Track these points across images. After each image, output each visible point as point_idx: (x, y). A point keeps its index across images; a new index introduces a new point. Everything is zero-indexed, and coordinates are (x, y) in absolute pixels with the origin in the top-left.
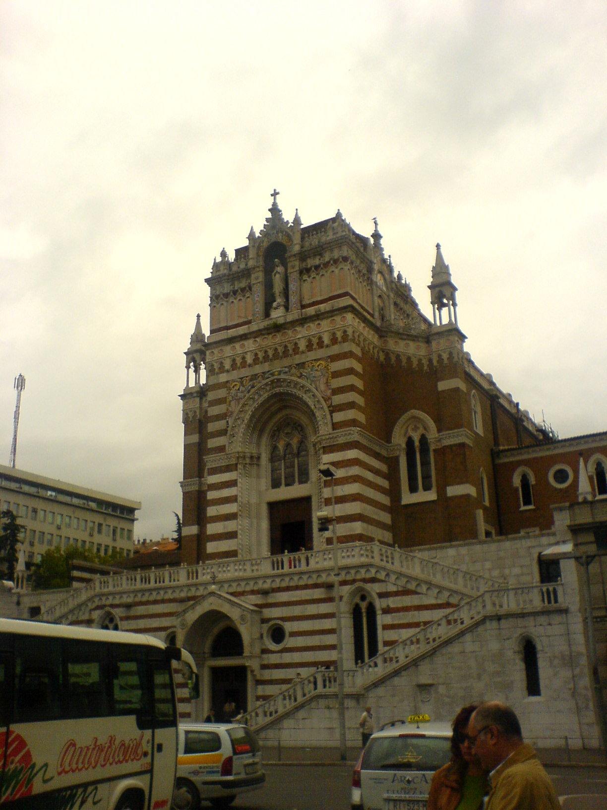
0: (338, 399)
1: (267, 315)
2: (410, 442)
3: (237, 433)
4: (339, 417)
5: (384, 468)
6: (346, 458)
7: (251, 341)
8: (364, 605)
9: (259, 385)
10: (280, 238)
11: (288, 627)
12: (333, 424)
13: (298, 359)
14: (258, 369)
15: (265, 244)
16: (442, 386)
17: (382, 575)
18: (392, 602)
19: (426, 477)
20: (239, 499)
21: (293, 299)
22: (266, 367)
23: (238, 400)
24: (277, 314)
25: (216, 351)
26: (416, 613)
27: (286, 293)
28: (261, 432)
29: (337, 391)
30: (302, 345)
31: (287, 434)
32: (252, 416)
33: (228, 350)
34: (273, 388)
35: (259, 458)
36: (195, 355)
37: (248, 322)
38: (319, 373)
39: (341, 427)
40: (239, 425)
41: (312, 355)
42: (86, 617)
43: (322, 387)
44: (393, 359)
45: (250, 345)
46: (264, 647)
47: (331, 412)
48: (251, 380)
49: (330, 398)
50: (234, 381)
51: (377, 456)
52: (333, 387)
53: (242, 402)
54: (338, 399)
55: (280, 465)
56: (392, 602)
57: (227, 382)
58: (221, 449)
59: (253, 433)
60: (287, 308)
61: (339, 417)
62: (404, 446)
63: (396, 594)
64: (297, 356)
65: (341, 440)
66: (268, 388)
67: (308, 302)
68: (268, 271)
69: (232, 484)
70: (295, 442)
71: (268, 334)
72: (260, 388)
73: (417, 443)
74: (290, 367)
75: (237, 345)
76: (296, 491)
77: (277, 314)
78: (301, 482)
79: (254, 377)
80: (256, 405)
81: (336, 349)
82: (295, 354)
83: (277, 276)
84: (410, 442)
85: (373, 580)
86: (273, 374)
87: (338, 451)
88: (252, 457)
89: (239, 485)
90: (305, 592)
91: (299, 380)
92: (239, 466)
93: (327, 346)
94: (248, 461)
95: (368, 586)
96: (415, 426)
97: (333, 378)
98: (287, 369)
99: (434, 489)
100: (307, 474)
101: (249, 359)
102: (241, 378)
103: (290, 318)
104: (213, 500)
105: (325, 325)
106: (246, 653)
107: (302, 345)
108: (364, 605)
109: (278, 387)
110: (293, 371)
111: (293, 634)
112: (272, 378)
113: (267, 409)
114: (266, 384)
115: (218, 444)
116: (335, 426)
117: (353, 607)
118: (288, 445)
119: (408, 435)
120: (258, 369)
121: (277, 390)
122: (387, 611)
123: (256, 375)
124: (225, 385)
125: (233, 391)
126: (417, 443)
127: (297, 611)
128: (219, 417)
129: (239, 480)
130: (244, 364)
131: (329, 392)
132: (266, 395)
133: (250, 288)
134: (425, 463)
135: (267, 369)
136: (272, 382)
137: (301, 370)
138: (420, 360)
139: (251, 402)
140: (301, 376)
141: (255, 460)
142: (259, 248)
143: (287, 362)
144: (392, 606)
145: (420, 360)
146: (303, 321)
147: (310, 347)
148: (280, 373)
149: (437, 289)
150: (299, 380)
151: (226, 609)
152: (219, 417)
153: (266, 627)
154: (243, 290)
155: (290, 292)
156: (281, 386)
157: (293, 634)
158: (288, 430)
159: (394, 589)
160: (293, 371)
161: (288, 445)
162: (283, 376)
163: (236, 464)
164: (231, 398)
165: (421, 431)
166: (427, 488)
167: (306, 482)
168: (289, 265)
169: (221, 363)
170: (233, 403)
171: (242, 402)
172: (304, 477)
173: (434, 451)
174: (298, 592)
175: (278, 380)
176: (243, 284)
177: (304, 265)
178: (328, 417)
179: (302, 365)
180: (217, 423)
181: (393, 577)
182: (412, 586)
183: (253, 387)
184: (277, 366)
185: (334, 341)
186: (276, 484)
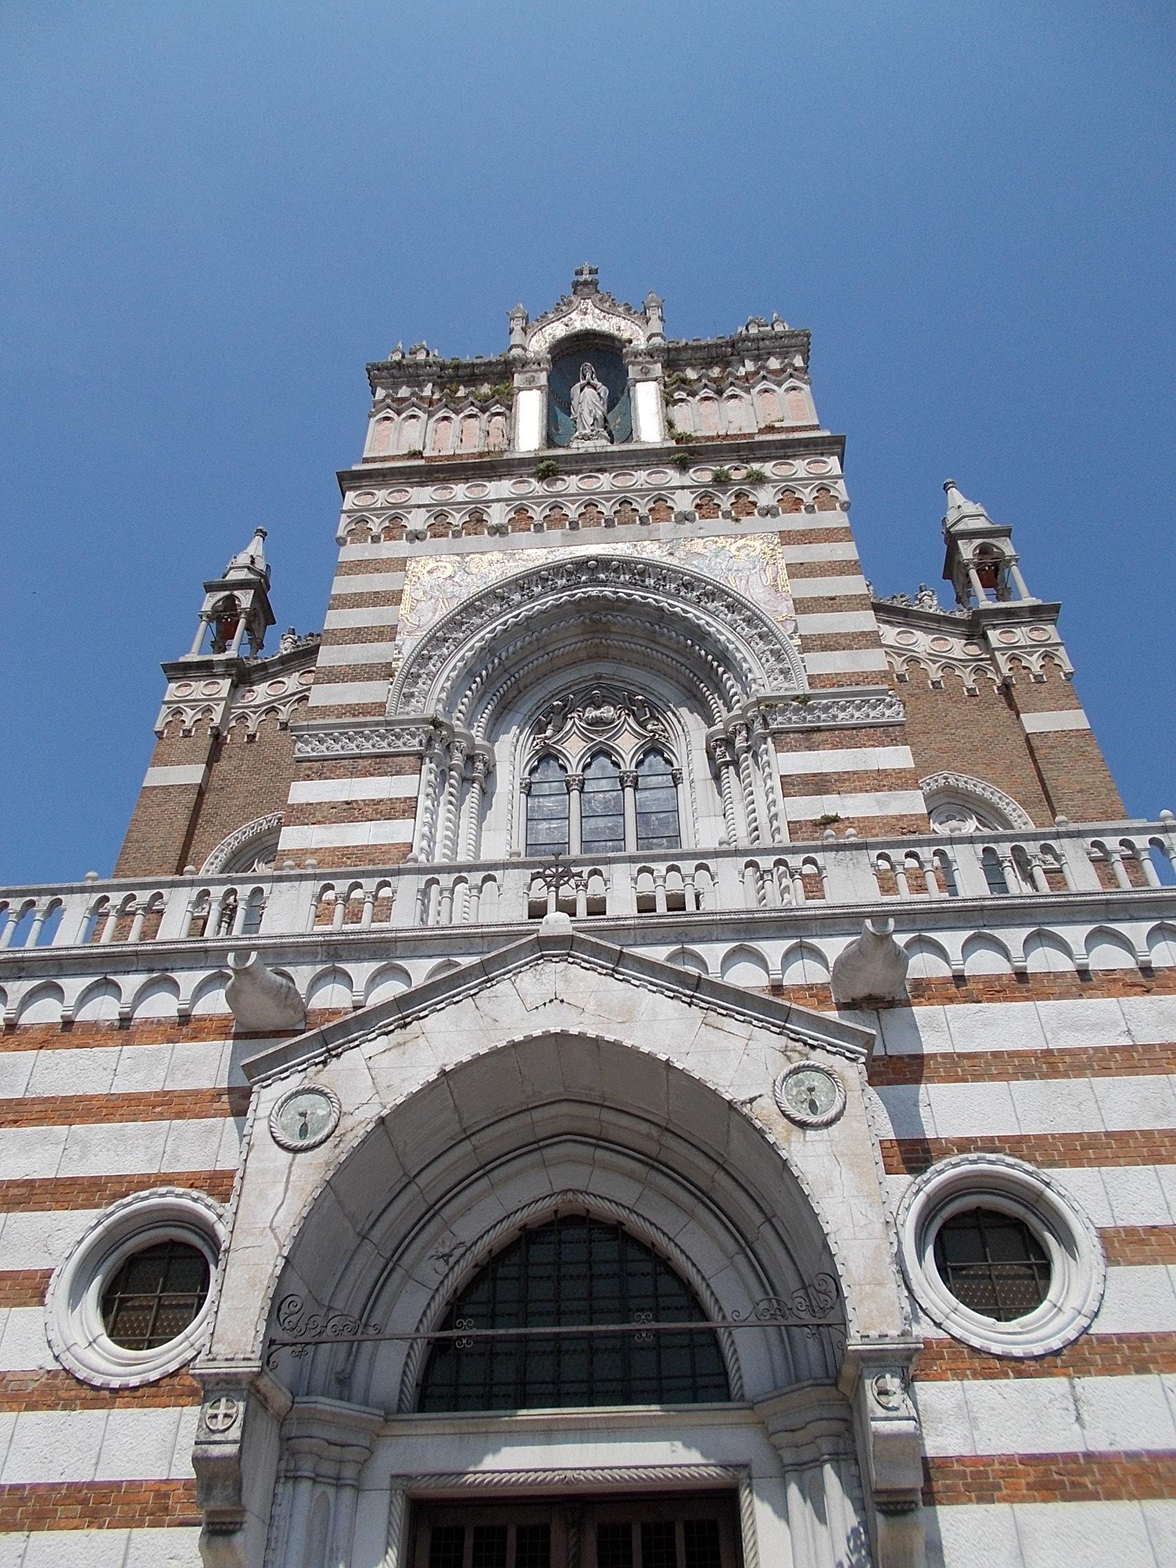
3: (432, 676)
11: (1085, 1197)
16: (1033, 722)
31: (598, 722)
34: (578, 585)
40: (443, 659)
59: (480, 698)
80: (509, 618)
88: (470, 759)
92: (428, 765)
94: (458, 759)
111: (1125, 1245)
121: (594, 591)
127: (1123, 1103)
129: (423, 803)
149: (979, 541)
151: (657, 1026)
153: (908, 1195)
156: (603, 583)
157: (1125, 1245)
158: (607, 712)
163: (421, 757)
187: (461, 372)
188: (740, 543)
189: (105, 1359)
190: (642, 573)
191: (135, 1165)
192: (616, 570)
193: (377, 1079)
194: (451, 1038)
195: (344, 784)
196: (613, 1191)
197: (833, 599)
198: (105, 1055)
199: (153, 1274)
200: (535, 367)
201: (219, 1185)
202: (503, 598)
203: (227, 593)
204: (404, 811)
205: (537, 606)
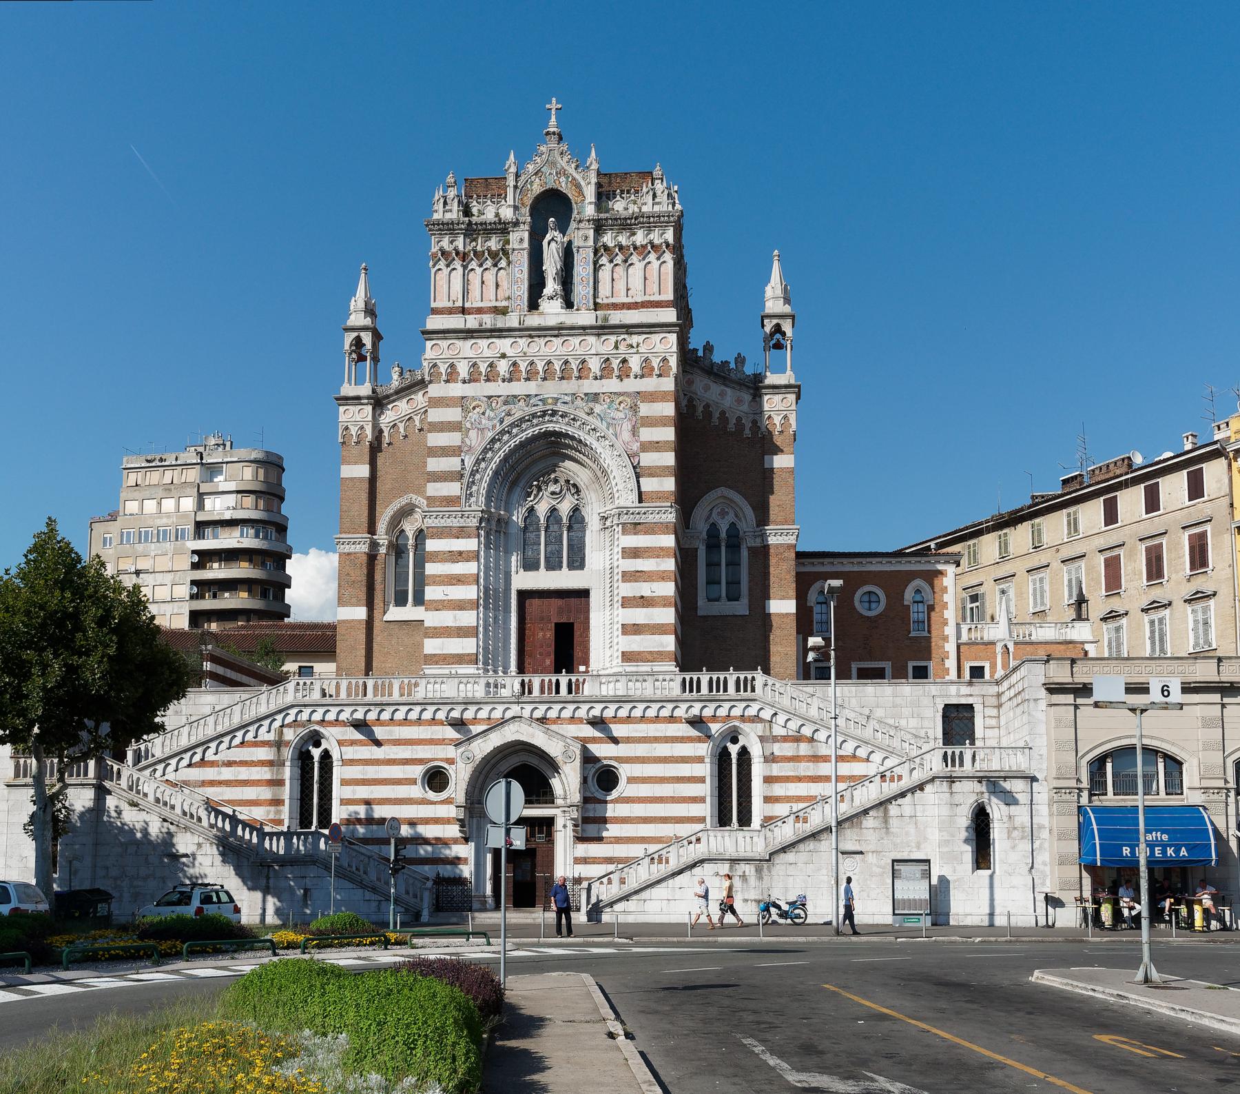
1: (533, 305)
2: (713, 531)
8: (734, 750)
11: (624, 771)
12: (640, 493)
13: (589, 386)
14: (518, 388)
17: (766, 714)
18: (778, 749)
19: (734, 583)
21: (581, 290)
22: (532, 388)
26: (811, 764)
27: (566, 279)
31: (553, 493)
32: (505, 459)
33: (466, 348)
36: (362, 334)
38: (621, 415)
41: (612, 385)
42: (271, 737)
43: (626, 436)
46: (588, 794)
47: (638, 476)
48: (506, 403)
49: (636, 455)
53: (490, 435)
54: (647, 459)
55: (539, 537)
56: (778, 749)
57: (463, 398)
60: (569, 304)
62: (704, 535)
63: (785, 739)
65: (651, 518)
67: (606, 301)
68: (536, 237)
70: (565, 508)
72: (522, 420)
73: (723, 535)
76: (564, 579)
77: (552, 311)
78: (571, 567)
79: (511, 400)
80: (512, 444)
81: (649, 384)
84: (713, 531)
85: (756, 719)
86: (544, 401)
87: (645, 533)
90: (652, 726)
95: (746, 727)
96: (723, 510)
97: (643, 425)
98: (568, 399)
99: (745, 600)
100: (583, 559)
102: (489, 397)
106: (559, 802)
108: (734, 750)
110: (579, 402)
111: (631, 780)
114: (534, 416)
117: (719, 750)
118: (553, 510)
119: (711, 521)
120: (518, 388)
122: (770, 759)
123: (515, 397)
124: (462, 401)
125: (474, 415)
126: (723, 535)
128: (445, 452)
131: (635, 447)
134: (733, 564)
136: (544, 413)
137: (591, 405)
138: (739, 419)
140: (590, 413)
144: (777, 753)
145: (739, 419)
147: (606, 371)
149: (775, 321)
150: (590, 418)
152: (445, 452)
154: (494, 255)
155: (576, 279)
156: (557, 422)
157: (631, 780)
159: (783, 732)
160: (579, 402)
161: (553, 510)
162: (560, 407)
164: (468, 425)
165: (731, 518)
166: (733, 597)
167: (581, 566)
169: (452, 366)
170: (473, 434)
172: (578, 562)
173: (749, 549)
174: (642, 726)
175: (554, 413)
179: (595, 397)
181: (781, 719)
182: (807, 731)
183: (509, 414)
184: (552, 389)
188: (621, 399)
189: (431, 795)
190: (574, 419)
191: (429, 756)
192: (562, 416)
193: (483, 748)
194: (496, 740)
196: (534, 761)
198: (415, 728)
199: (436, 779)
201: (451, 761)
205: (523, 436)
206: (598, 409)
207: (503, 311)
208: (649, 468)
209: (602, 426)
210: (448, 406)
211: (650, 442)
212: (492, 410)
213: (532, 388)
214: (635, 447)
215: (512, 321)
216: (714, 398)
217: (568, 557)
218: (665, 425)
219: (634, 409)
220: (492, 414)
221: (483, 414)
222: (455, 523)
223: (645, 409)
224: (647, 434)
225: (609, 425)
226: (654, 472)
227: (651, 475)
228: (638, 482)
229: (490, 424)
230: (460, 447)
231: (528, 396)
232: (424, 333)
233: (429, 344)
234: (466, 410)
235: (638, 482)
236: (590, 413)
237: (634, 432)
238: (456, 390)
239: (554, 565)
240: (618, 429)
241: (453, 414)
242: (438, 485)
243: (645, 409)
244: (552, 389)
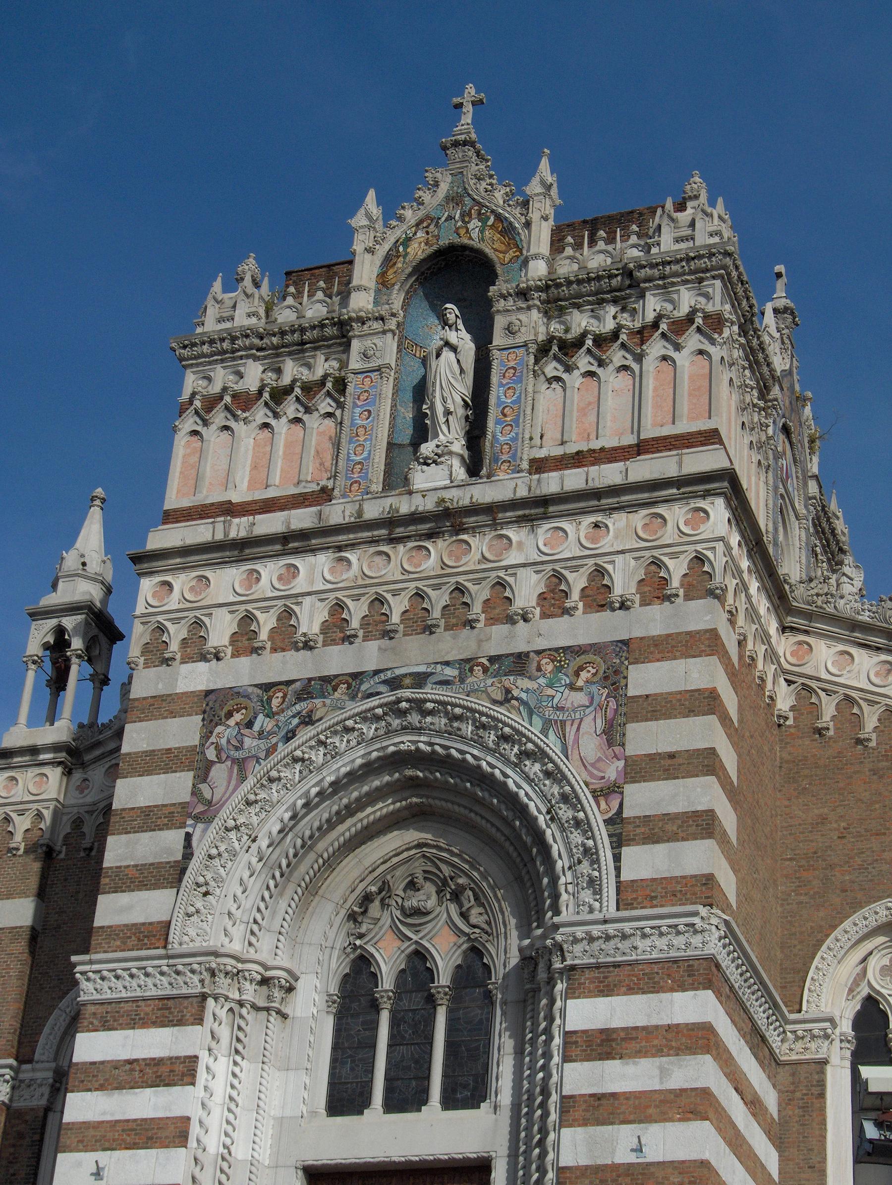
0: (643, 799)
4: (643, 862)
5: (771, 1099)
6: (665, 1020)
7: (323, 561)
9: (338, 716)
10: (477, 235)
13: (500, 640)
15: (418, 250)
20: (195, 1130)
23: (241, 765)
24: (437, 480)
25: (181, 582)
28: (311, 890)
29: (644, 769)
30: (527, 590)
33: (226, 581)
35: (290, 989)
37: (324, 495)
38: (580, 698)
39: (652, 900)
43: (590, 744)
44: (829, 708)
45: (315, 569)
47: (618, 842)
50: (233, 693)
51: (757, 1040)
52: (631, 750)
54: (643, 799)
55: (374, 1026)
57: (208, 693)
58: (157, 934)
61: (643, 862)
62: (846, 1027)
64: (499, 630)
66: (369, 730)
69: (179, 1071)
71: (393, 541)
74: (467, 664)
75: (269, 571)
82: (492, 621)
83: (448, 355)
86: (394, 683)
87: (631, 990)
89: (202, 1076)
91: (501, 712)
93: (623, 606)
98: (450, 672)
101: (311, 619)
102: (267, 687)
103: (485, 493)
104: (86, 1125)
105: (623, 528)
107: (527, 590)
109: (407, 729)
110: (477, 678)
112: (389, 697)
113: (351, 810)
115: (137, 917)
116: (630, 894)
120: (337, 660)
121: (406, 742)
123: (326, 680)
128: (151, 819)
130: (287, 637)
131: (613, 771)
132: (356, 757)
133: (341, 385)
135: (371, 667)
137: (509, 681)
139: (291, 773)
141: (276, 986)
142: (389, 260)
143: (453, 645)
146: (536, 509)
148: (420, 680)
150: (501, 712)
152: (151, 819)
156: (419, 730)
162: (430, 692)
163: (204, 997)
168: (500, 322)
170: (219, 773)
171: (255, 772)
175: (418, 705)
176: (323, 365)
177: (556, 328)
178: (606, 855)
180: (145, 837)
183: (308, 720)
185: (655, 589)
186: (345, 1098)
187: (289, 338)
195: (126, 1037)
197: (672, 756)
200: (377, 325)
202: (303, 760)
203: (53, 622)
204: (183, 1075)
206: (521, 686)
207: (324, 495)
208: (646, 819)
209: (533, 729)
210: (173, 714)
211: (651, 757)
212: (270, 715)
213: (369, 655)
214: (613, 771)
215: (338, 513)
216: (864, 684)
217: (445, 1075)
218: (691, 712)
219: (613, 680)
220: (269, 725)
221: (250, 725)
222: (157, 986)
223: (645, 679)
224: (646, 738)
225: (547, 725)
226: (658, 830)
227: (652, 839)
228: (617, 858)
229: (263, 745)
230: (184, 805)
231: (357, 676)
232: (137, 559)
233: (147, 585)
234: (211, 721)
235: (617, 858)
236: (507, 698)
237: (612, 735)
238: (195, 678)
239: (405, 1097)
240: (571, 732)
241: (183, 732)
242: (124, 899)
243: (645, 679)
244: (414, 654)
